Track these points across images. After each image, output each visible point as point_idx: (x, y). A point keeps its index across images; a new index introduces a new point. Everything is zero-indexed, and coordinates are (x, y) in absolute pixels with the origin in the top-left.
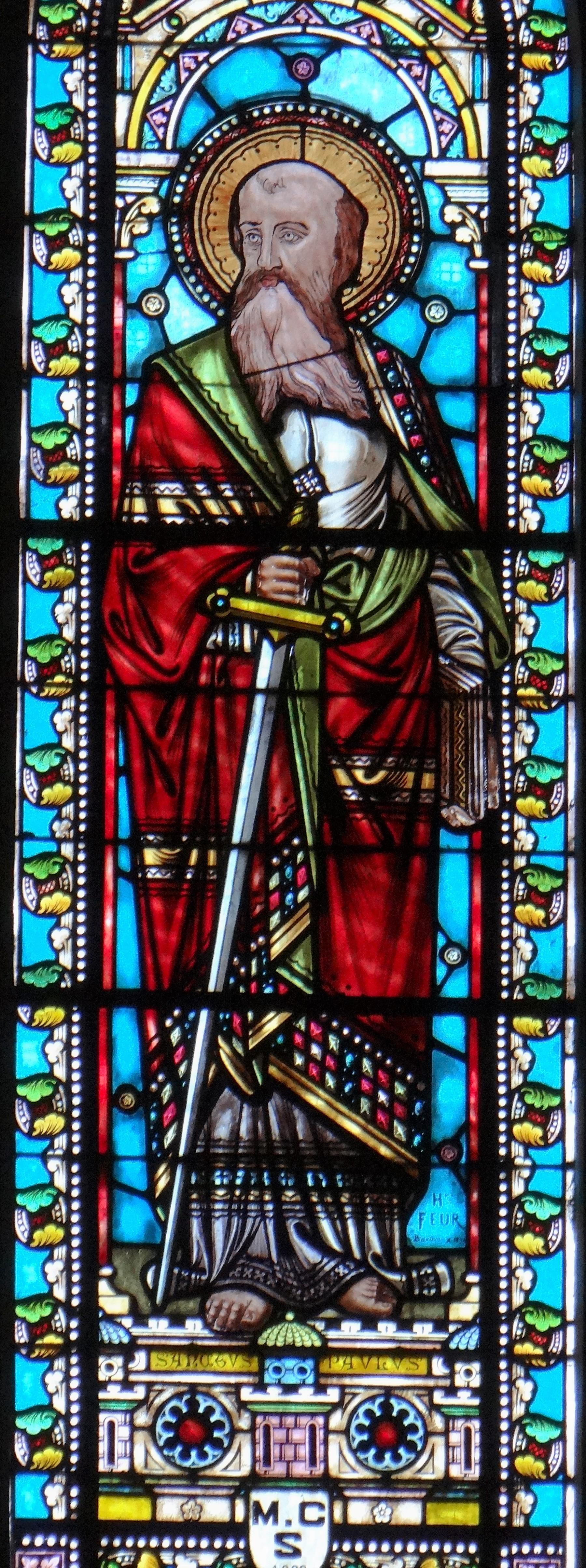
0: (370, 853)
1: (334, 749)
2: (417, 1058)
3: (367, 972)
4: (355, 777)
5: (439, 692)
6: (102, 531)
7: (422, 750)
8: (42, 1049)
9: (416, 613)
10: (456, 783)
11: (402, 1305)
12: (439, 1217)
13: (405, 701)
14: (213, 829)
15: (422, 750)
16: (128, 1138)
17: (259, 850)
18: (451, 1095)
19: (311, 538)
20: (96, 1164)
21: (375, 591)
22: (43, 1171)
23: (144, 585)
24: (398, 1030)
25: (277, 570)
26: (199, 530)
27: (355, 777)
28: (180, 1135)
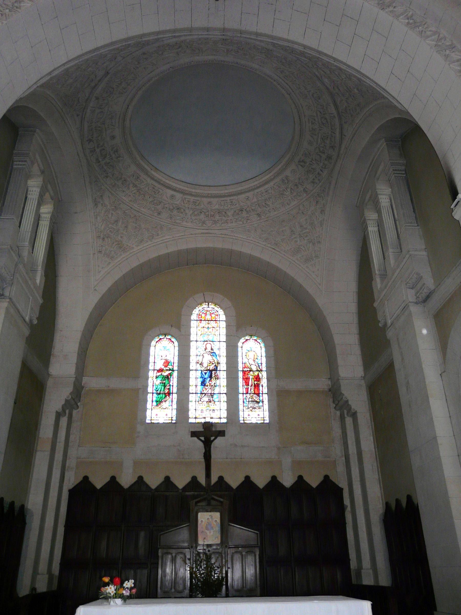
0: (257, 386)
1: (254, 381)
2: (259, 396)
3: (256, 392)
4: (256, 382)
5: (259, 378)
6: (243, 371)
7: (259, 381)
8: (241, 396)
9: (258, 375)
10: (260, 382)
11: (259, 408)
12: (261, 404)
13: (258, 378)
14: (248, 385)
15: (259, 381)
16: (245, 401)
17: (251, 386)
18: (261, 398)
19: (253, 371)
20: (244, 402)
21: (256, 373)
22: (241, 402)
23: (245, 373)
24: (258, 394)
25: (251, 372)
26: (248, 371)
27: (256, 382)
28: (248, 400)
